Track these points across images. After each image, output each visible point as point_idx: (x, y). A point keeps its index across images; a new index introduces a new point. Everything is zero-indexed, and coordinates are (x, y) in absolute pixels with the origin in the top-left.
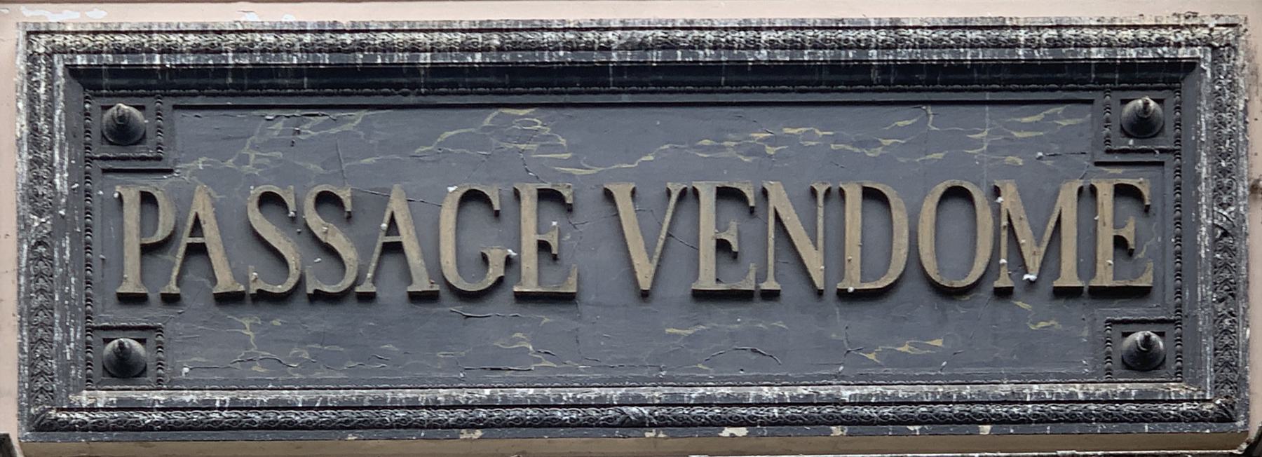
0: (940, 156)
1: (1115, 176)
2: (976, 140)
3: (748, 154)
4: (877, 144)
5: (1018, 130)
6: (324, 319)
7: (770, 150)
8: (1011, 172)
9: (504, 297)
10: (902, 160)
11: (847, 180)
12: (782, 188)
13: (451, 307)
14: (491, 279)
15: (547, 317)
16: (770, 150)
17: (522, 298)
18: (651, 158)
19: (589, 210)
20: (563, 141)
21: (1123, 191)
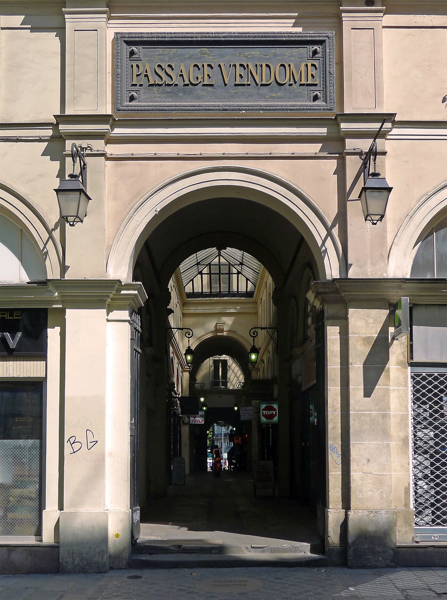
0: (279, 58)
1: (311, 62)
2: (286, 55)
3: (245, 57)
4: (268, 55)
5: (294, 53)
6: (168, 89)
7: (249, 56)
8: (292, 61)
9: (201, 84)
10: (273, 58)
11: (263, 62)
12: (251, 64)
13: (190, 86)
14: (199, 81)
15: (209, 88)
16: (249, 56)
17: (204, 85)
18: (228, 58)
19: (216, 68)
20: (212, 55)
21: (313, 65)
